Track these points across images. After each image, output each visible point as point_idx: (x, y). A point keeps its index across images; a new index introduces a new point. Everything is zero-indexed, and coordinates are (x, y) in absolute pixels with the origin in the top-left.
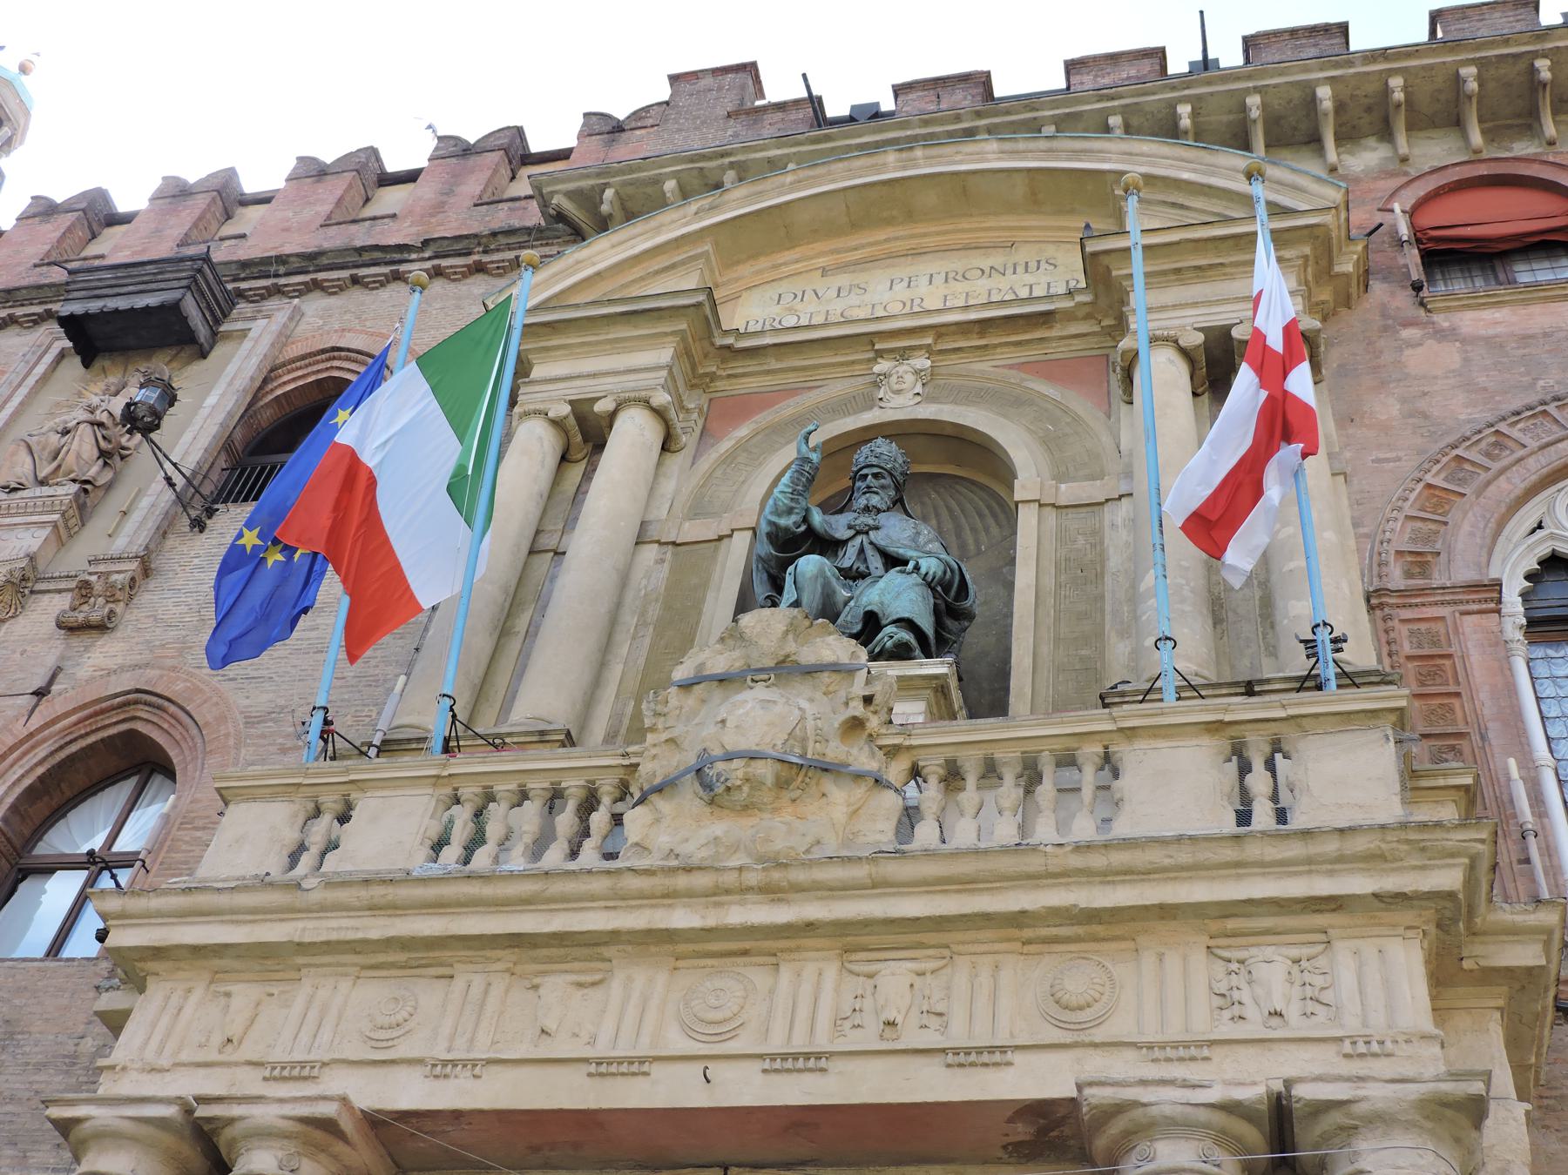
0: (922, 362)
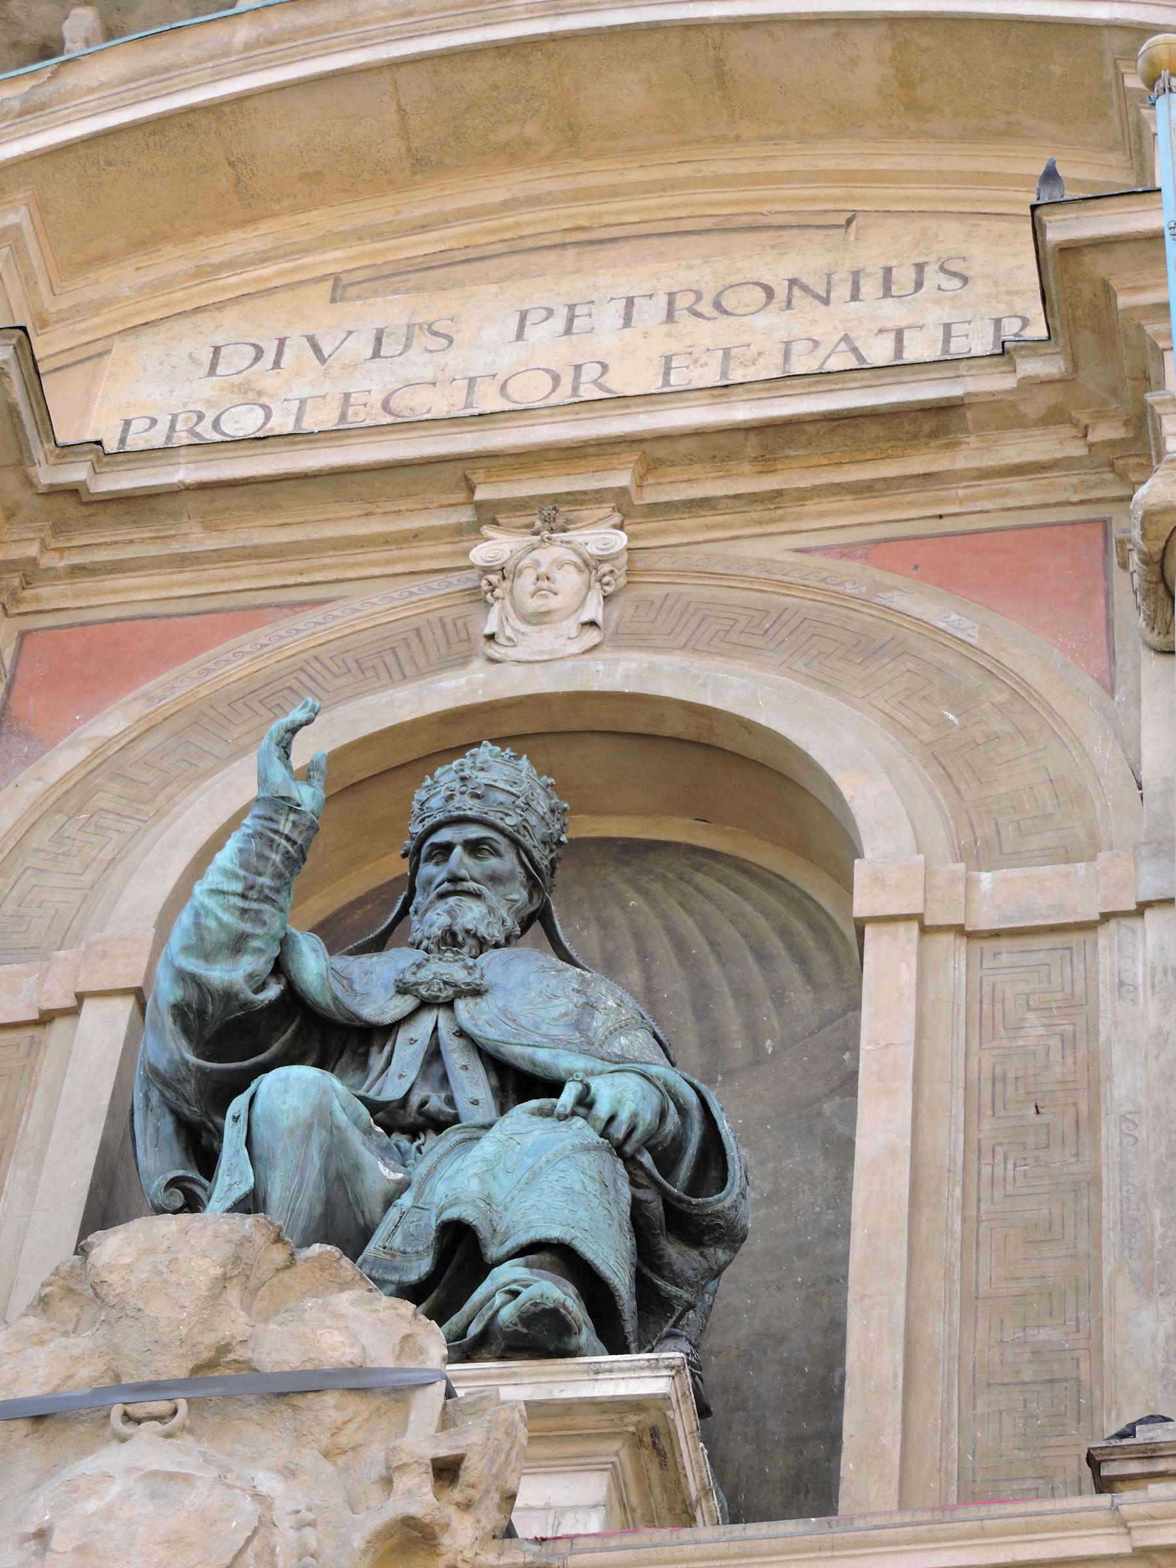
0: (602, 537)
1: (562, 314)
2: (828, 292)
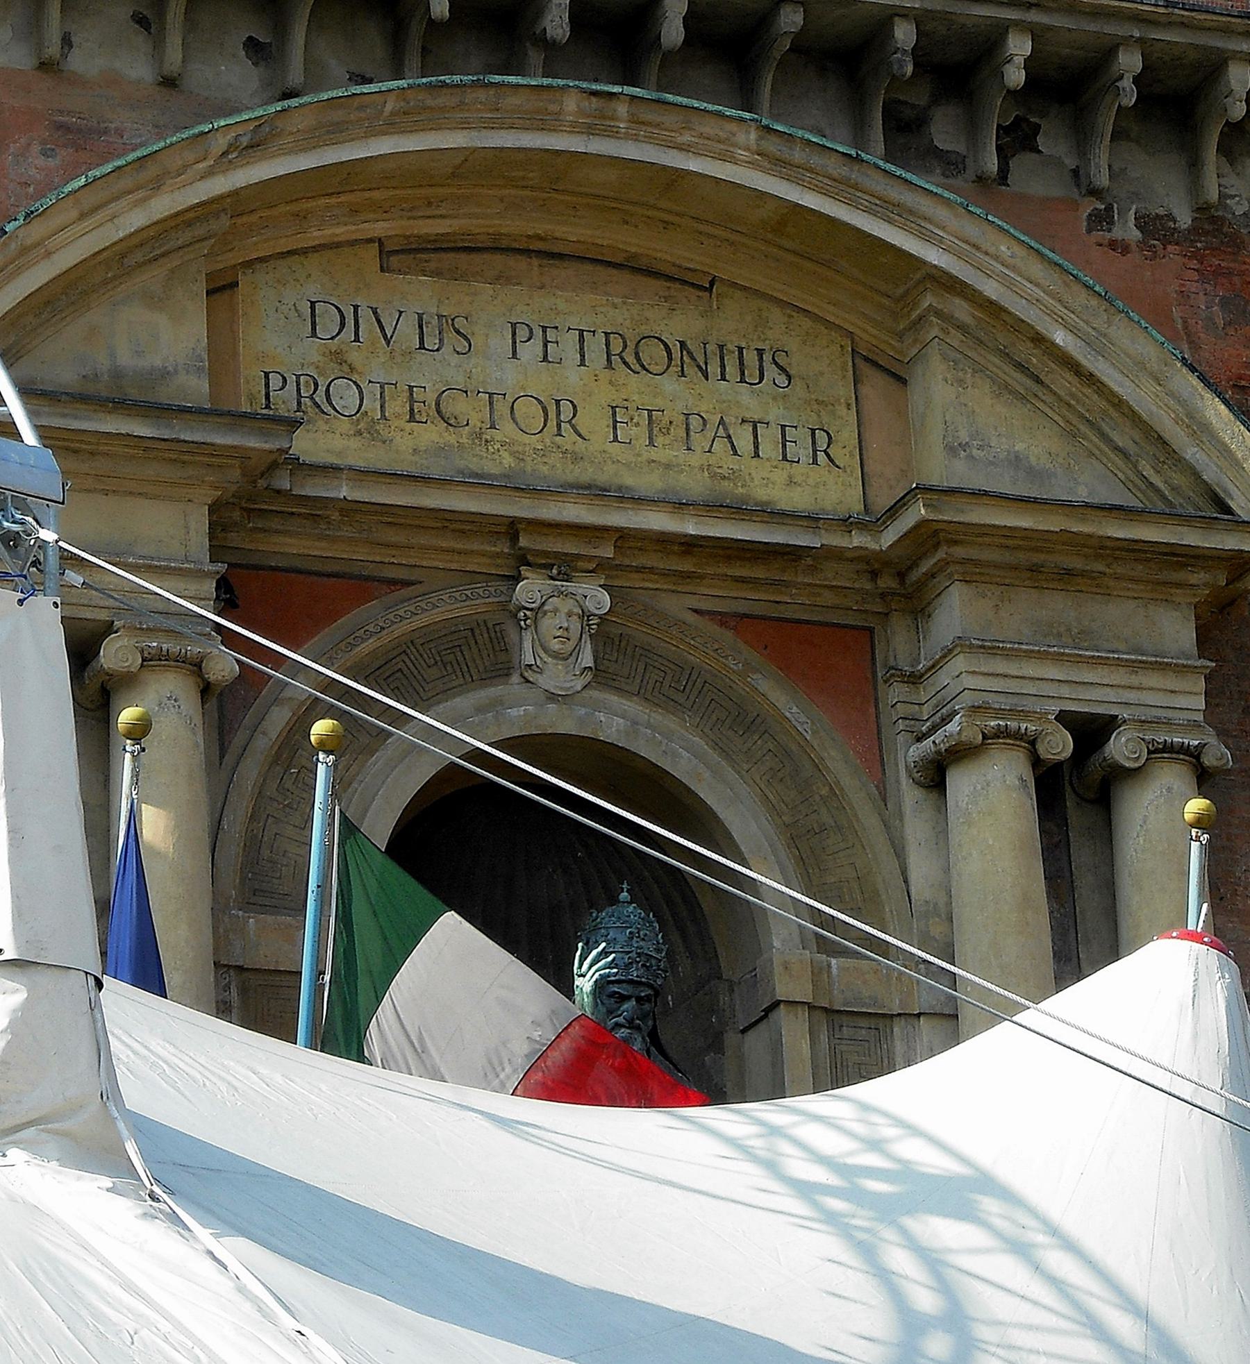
0: (599, 601)
1: (538, 332)
2: (706, 364)
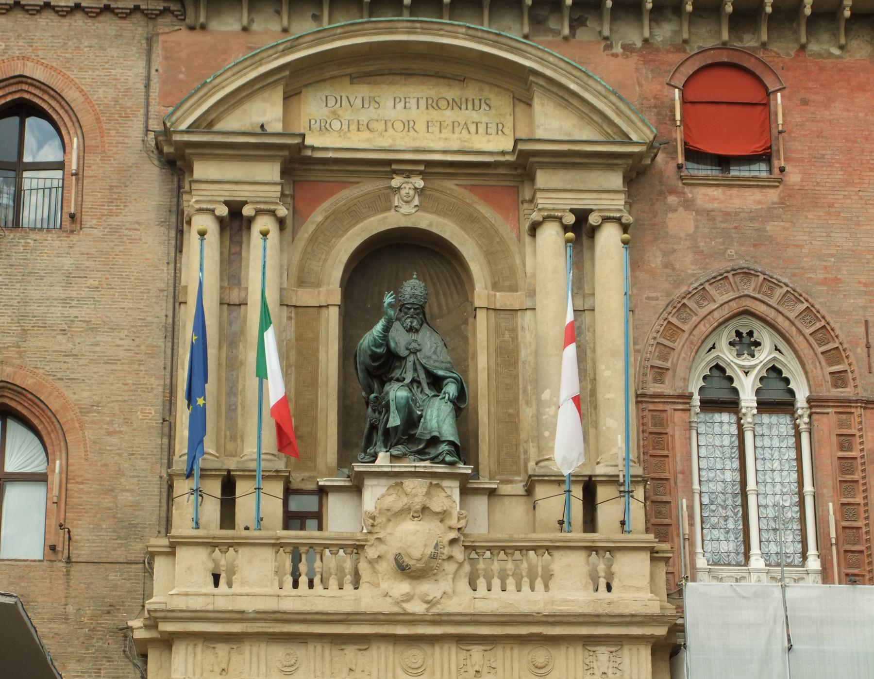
0: (419, 183)
1: (403, 100)
